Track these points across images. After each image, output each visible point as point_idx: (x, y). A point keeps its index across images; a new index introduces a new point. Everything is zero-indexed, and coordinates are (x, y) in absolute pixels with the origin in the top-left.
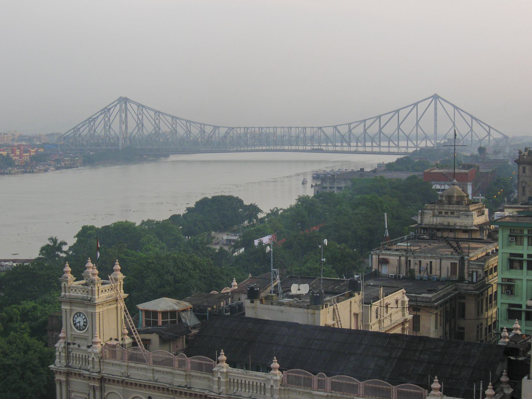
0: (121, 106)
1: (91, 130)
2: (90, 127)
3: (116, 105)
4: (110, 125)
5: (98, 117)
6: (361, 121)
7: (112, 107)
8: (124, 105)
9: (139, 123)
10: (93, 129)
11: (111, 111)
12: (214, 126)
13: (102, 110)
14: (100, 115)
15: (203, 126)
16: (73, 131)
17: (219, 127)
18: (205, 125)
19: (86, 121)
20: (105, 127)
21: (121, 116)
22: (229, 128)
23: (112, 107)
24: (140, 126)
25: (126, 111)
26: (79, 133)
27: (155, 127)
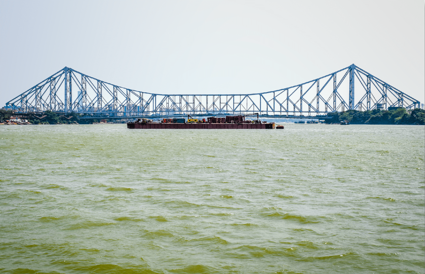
0: (66, 75)
1: (37, 96)
2: (37, 94)
3: (61, 75)
4: (55, 93)
5: (44, 85)
6: (285, 89)
7: (58, 77)
8: (68, 75)
9: (83, 91)
10: (40, 96)
11: (57, 80)
12: (152, 94)
13: (48, 79)
14: (47, 83)
15: (141, 93)
16: (20, 97)
17: (155, 95)
18: (143, 93)
19: (33, 88)
20: (51, 94)
21: (66, 84)
22: (165, 95)
23: (58, 77)
24: (84, 93)
25: (70, 80)
26: (25, 100)
27: (98, 94)
